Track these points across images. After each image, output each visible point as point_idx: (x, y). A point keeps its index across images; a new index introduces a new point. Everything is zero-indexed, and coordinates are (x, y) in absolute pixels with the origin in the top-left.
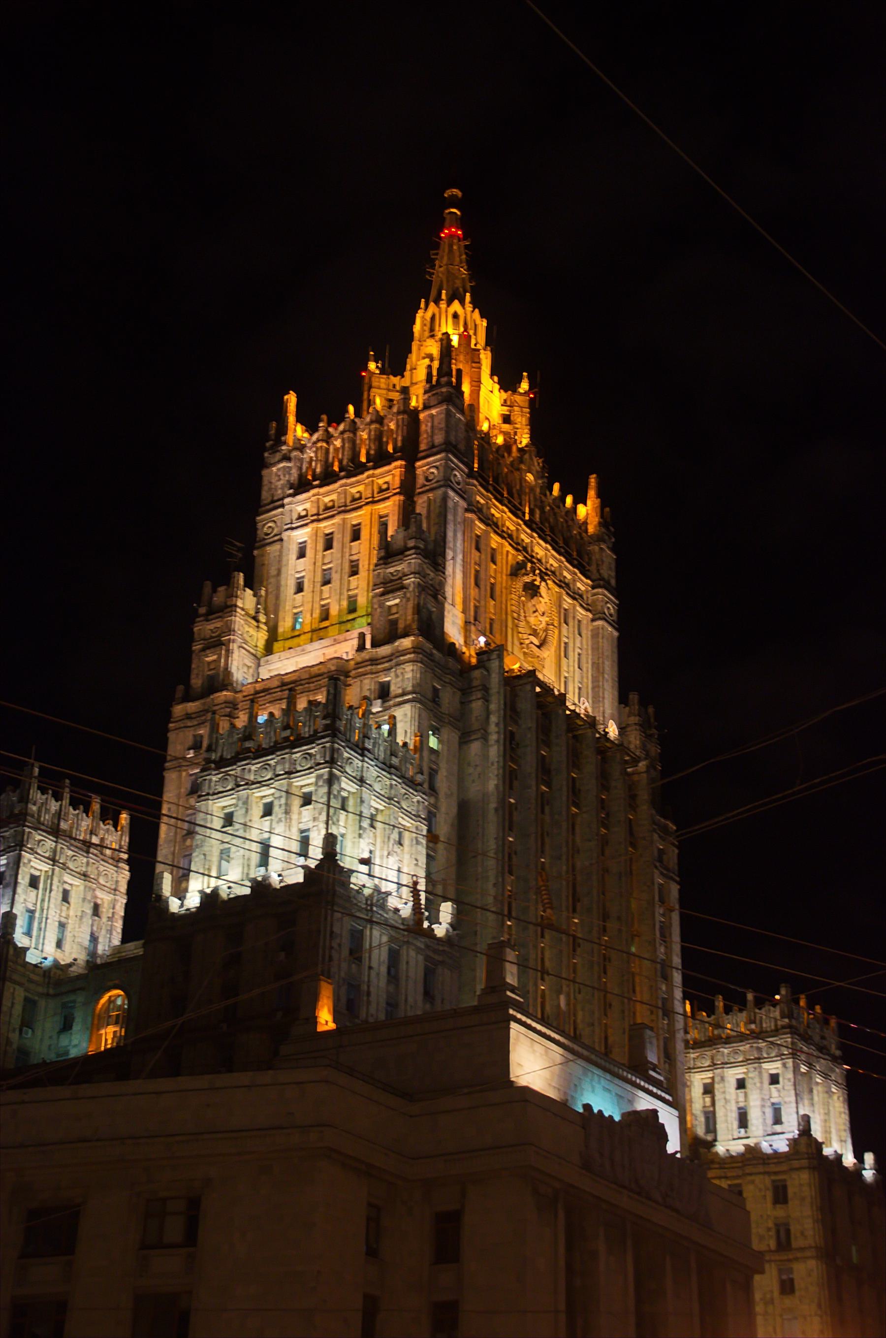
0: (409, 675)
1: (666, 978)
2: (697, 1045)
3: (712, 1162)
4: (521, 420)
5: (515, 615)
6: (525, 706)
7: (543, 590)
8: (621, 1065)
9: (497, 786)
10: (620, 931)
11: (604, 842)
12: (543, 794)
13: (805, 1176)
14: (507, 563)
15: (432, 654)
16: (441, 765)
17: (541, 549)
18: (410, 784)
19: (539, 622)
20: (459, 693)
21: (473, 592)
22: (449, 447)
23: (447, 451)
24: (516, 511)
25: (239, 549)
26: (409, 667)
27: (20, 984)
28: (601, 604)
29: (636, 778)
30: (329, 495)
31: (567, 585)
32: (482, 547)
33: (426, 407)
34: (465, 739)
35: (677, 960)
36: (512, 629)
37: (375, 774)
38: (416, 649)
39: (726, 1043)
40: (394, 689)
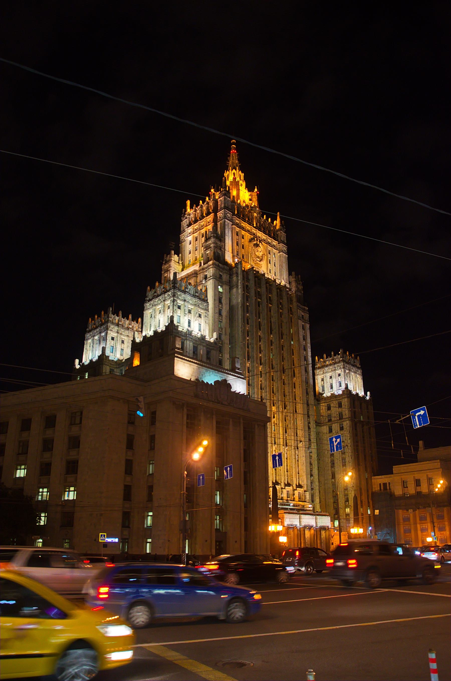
0: (211, 271)
1: (305, 349)
2: (319, 368)
3: (323, 399)
4: (255, 199)
6: (251, 277)
7: (260, 245)
8: (227, 370)
9: (241, 300)
10: (287, 338)
11: (281, 314)
12: (259, 302)
13: (346, 399)
15: (218, 265)
17: (260, 234)
19: (260, 254)
20: (228, 276)
21: (235, 247)
22: (226, 208)
23: (224, 209)
24: (251, 224)
25: (174, 244)
26: (211, 269)
27: (108, 365)
29: (292, 295)
30: (196, 226)
31: (270, 243)
32: (239, 234)
33: (219, 198)
34: (231, 288)
35: (309, 345)
37: (190, 298)
38: (213, 264)
40: (208, 276)
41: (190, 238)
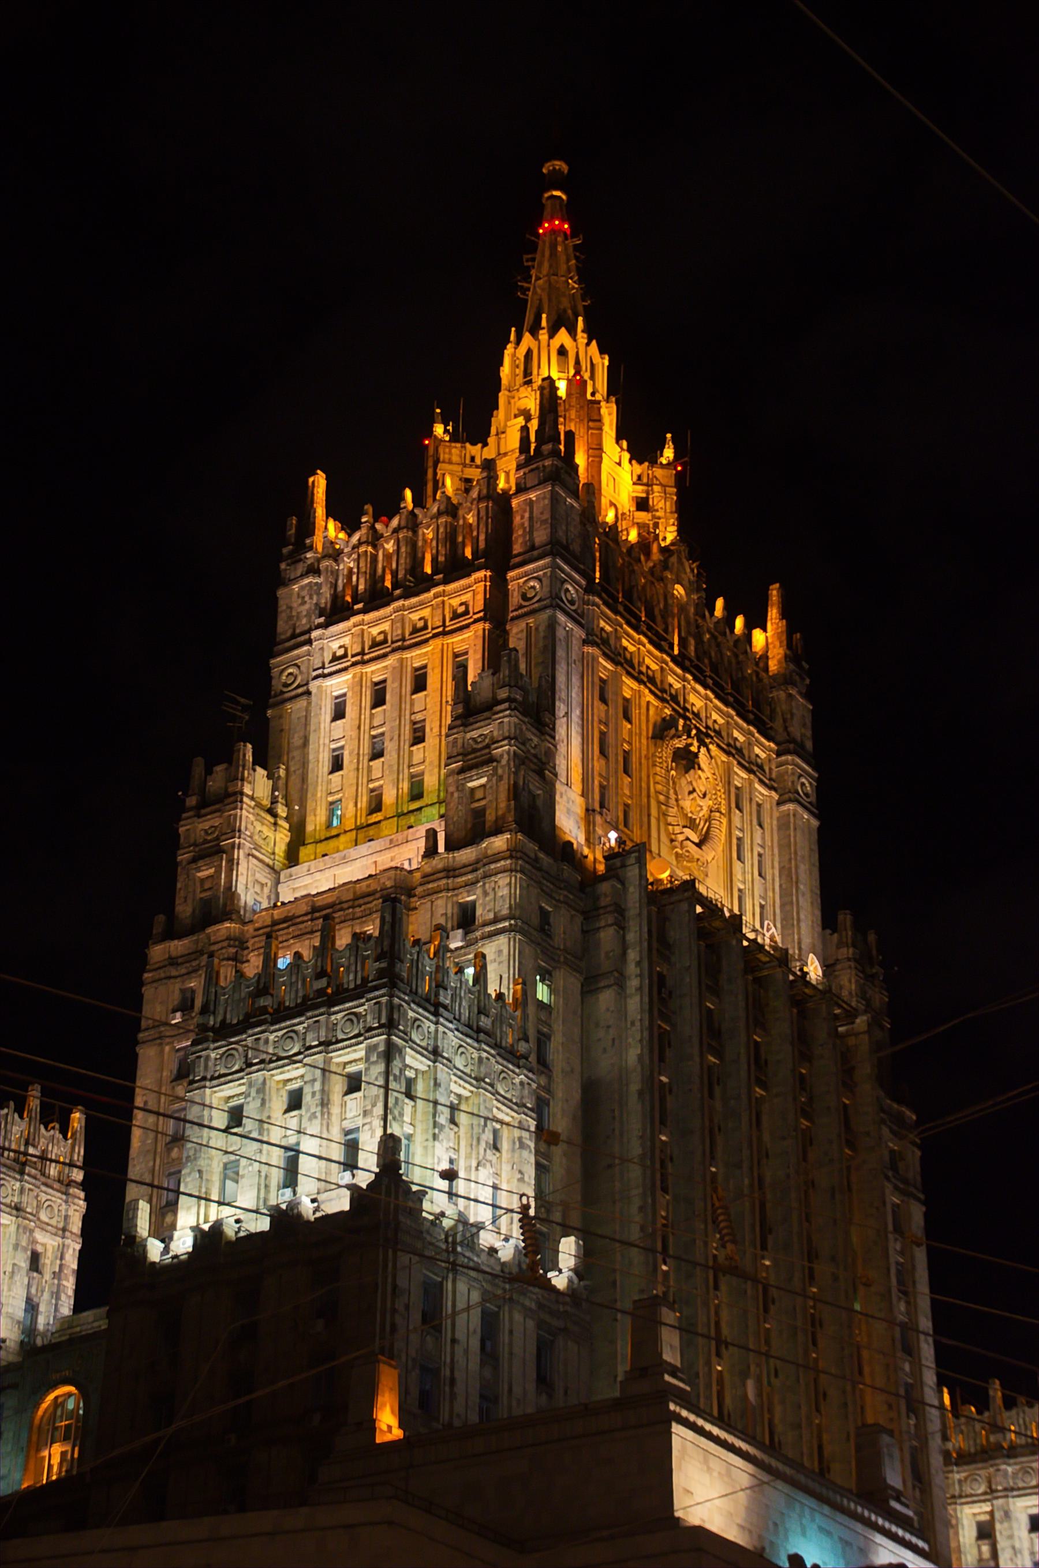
1: (910, 1350)
2: (964, 1459)
4: (663, 503)
5: (662, 798)
6: (680, 934)
7: (703, 758)
9: (640, 1057)
10: (835, 1278)
12: (710, 1068)
14: (648, 721)
15: (537, 859)
16: (555, 1027)
17: (698, 699)
18: (510, 1057)
19: (697, 807)
20: (579, 919)
21: (598, 764)
22: (556, 548)
23: (552, 554)
24: (660, 642)
25: (245, 708)
26: (503, 880)
28: (791, 779)
29: (852, 1041)
30: (378, 623)
31: (740, 751)
32: (610, 696)
33: (521, 489)
34: (590, 986)
35: (925, 1323)
36: (658, 820)
37: (456, 1042)
38: (513, 852)
39: (1009, 1457)
41: (338, 685)
